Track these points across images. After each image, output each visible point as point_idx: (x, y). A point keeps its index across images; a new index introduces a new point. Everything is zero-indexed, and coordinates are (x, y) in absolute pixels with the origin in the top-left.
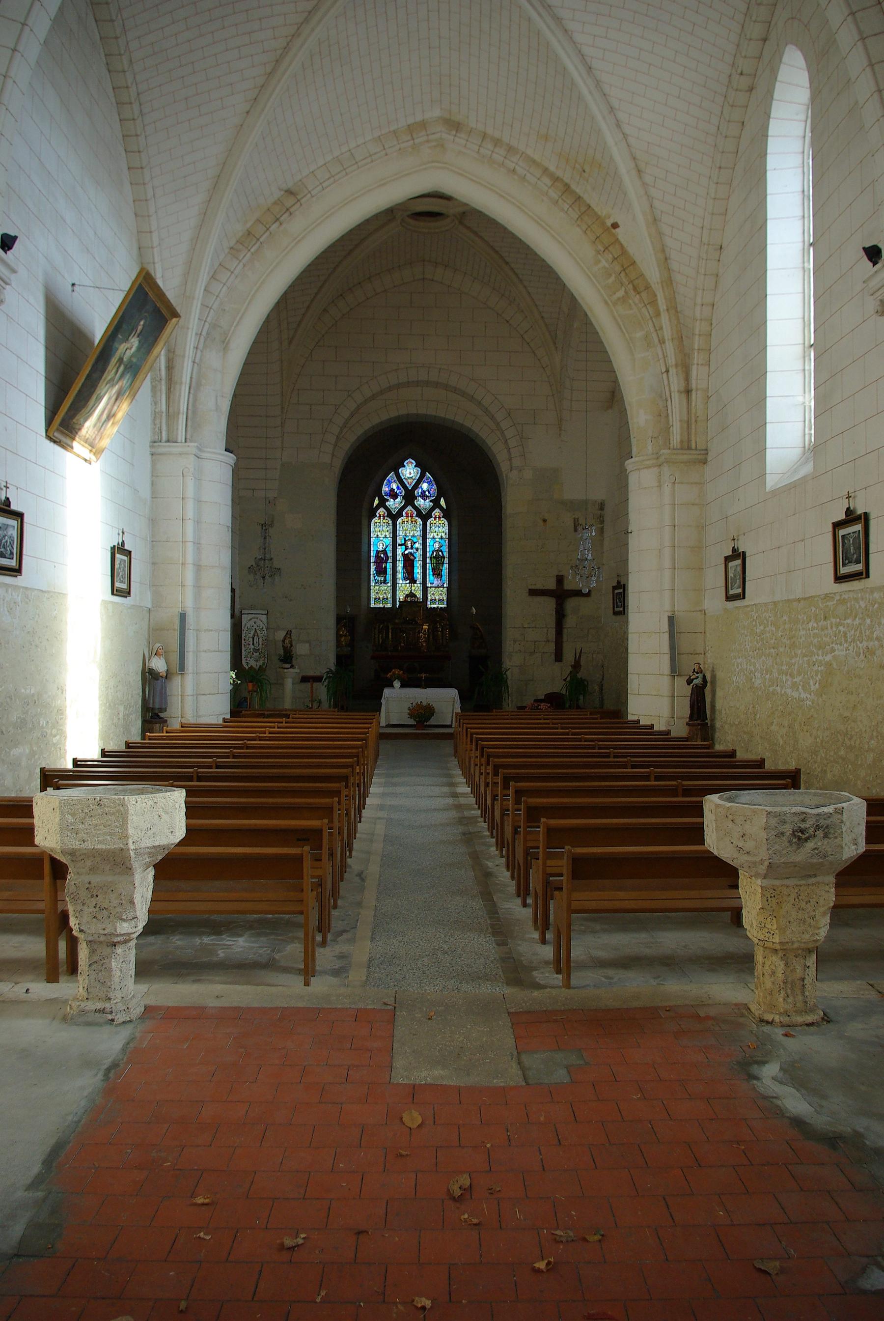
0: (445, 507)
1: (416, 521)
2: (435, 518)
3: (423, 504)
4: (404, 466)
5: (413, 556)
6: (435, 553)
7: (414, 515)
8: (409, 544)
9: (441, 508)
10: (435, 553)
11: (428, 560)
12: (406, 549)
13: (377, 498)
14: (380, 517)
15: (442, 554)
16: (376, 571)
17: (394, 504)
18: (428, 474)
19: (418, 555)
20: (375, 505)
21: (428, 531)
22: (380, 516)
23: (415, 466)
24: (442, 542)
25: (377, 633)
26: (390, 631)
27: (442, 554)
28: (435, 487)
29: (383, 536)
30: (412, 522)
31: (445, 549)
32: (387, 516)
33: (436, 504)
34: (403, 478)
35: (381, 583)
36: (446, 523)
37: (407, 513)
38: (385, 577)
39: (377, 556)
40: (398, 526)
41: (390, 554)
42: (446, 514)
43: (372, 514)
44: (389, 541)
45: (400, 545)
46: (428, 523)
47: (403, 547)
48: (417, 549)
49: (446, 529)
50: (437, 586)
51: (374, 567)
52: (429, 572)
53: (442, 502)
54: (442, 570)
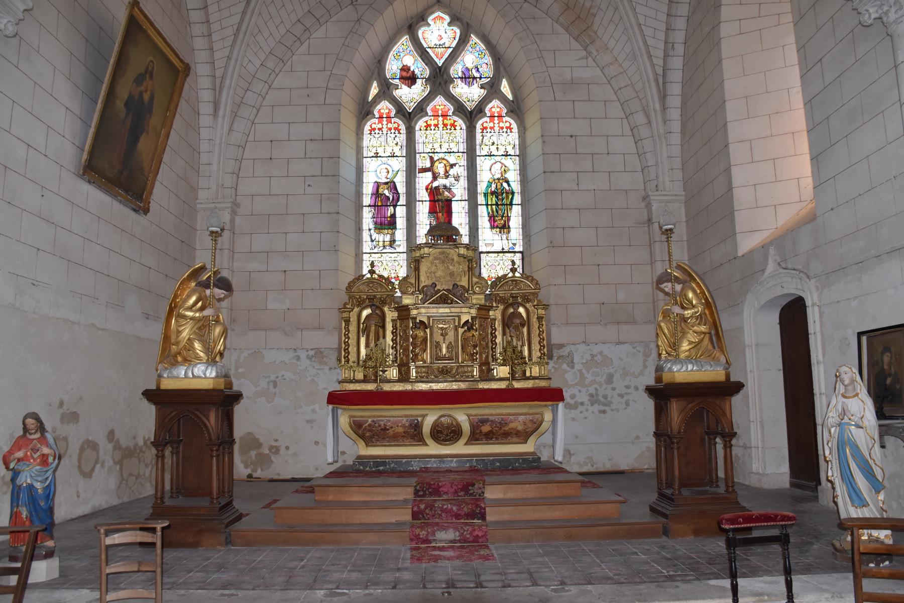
0: (510, 97)
1: (453, 125)
3: (469, 93)
4: (429, 25)
5: (449, 190)
6: (494, 186)
7: (450, 113)
8: (440, 168)
9: (503, 99)
10: (494, 186)
11: (481, 199)
13: (375, 84)
14: (381, 117)
15: (509, 185)
16: (376, 223)
17: (409, 95)
18: (474, 39)
19: (460, 190)
20: (370, 98)
21: (478, 141)
22: (381, 117)
23: (450, 24)
24: (508, 162)
25: (353, 335)
26: (389, 327)
27: (509, 185)
28: (488, 59)
29: (388, 154)
30: (445, 125)
31: (513, 176)
32: (396, 116)
33: (492, 89)
34: (425, 46)
35: (384, 247)
36: (514, 126)
37: (435, 110)
38: (393, 234)
39: (376, 194)
40: (418, 134)
41: (401, 189)
42: (515, 109)
43: (365, 111)
44: (399, 164)
46: (479, 126)
47: (429, 175)
48: (457, 178)
49: (514, 137)
50: (500, 249)
51: (371, 215)
52: (484, 221)
54: (509, 218)
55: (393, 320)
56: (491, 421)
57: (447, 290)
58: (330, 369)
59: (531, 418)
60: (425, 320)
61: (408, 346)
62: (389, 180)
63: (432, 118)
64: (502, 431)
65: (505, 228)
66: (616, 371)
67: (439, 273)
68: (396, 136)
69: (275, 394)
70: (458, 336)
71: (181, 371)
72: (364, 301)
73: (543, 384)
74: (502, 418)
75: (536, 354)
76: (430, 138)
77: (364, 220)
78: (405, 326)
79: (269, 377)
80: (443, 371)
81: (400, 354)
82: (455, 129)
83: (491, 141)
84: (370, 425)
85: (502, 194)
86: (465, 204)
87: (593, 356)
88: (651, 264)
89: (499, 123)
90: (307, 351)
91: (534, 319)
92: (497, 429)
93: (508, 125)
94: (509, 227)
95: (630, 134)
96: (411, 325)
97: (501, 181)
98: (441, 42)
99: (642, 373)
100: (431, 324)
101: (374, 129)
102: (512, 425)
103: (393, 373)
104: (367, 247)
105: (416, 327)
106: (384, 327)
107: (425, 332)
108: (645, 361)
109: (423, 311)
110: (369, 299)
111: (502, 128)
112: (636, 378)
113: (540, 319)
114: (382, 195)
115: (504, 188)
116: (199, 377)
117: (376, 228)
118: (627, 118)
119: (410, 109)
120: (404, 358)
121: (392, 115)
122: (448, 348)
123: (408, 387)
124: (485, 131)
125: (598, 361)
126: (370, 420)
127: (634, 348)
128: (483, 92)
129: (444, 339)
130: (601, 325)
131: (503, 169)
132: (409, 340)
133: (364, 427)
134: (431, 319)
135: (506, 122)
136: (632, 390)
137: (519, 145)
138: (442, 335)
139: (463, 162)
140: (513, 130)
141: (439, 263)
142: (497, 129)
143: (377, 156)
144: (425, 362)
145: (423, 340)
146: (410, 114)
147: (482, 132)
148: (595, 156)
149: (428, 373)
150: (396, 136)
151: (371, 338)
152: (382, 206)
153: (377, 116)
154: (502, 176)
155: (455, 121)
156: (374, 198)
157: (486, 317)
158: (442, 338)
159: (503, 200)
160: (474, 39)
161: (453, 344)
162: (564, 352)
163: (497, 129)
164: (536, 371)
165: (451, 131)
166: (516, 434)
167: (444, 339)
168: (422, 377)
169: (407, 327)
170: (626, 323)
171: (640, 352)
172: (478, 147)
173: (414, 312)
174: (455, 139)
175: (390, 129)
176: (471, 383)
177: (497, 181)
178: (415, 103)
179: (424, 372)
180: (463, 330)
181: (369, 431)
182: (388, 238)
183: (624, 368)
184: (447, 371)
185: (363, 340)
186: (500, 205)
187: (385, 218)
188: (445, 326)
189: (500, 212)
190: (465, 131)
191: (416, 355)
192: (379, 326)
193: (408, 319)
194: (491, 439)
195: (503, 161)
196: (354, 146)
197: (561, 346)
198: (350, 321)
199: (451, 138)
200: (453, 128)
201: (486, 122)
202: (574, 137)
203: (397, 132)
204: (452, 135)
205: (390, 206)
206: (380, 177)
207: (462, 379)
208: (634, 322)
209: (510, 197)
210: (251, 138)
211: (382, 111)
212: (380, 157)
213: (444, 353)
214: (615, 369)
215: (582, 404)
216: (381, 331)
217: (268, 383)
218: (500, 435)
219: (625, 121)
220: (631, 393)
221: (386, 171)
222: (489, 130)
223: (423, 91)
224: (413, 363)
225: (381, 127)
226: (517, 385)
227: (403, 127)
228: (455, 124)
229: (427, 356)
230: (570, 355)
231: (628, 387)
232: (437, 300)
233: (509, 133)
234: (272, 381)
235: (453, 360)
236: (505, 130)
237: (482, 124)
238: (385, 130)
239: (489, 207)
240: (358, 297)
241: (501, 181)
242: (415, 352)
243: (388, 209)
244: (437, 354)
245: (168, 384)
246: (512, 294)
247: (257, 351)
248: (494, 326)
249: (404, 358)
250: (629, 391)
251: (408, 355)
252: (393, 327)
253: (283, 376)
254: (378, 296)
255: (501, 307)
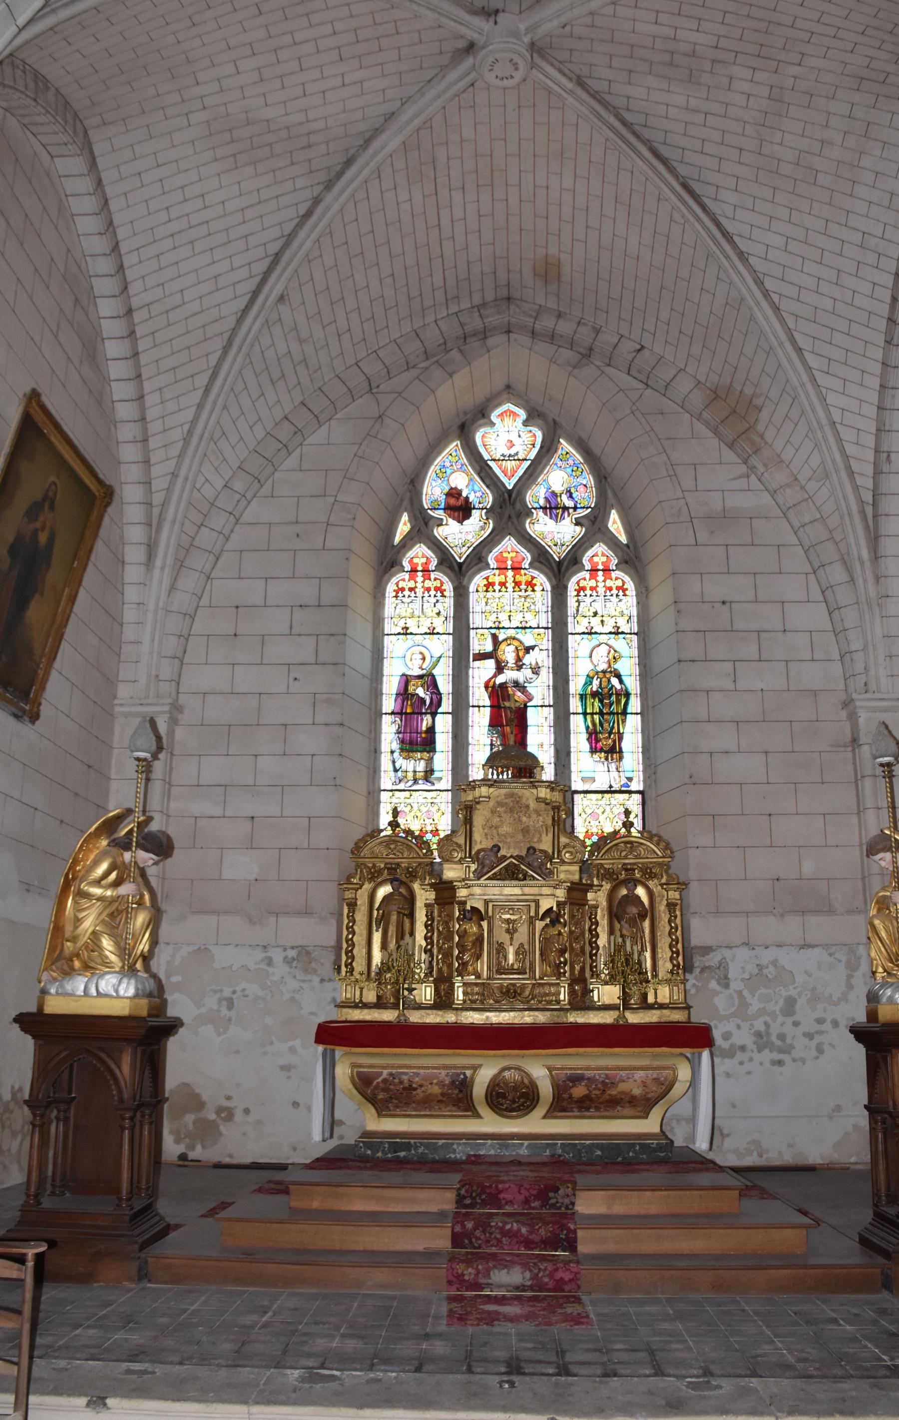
0: (623, 538)
1: (531, 584)
2: (594, 571)
4: (493, 424)
6: (596, 683)
8: (508, 654)
9: (612, 542)
10: (596, 683)
11: (575, 705)
12: (500, 669)
13: (405, 517)
14: (414, 571)
15: (621, 682)
16: (402, 742)
18: (565, 446)
20: (397, 539)
21: (571, 610)
22: (414, 571)
23: (526, 423)
24: (620, 644)
25: (360, 928)
27: (621, 682)
28: (588, 479)
30: (517, 584)
31: (629, 668)
32: (437, 568)
34: (486, 456)
35: (415, 781)
36: (630, 585)
37: (500, 560)
38: (430, 761)
39: (404, 694)
40: (473, 597)
41: (445, 686)
44: (443, 646)
45: (482, 656)
46: (572, 586)
47: (491, 664)
48: (536, 670)
49: (629, 604)
50: (605, 787)
51: (394, 728)
52: (579, 741)
53: (615, 524)
54: (620, 736)
55: (427, 905)
56: (589, 1079)
57: (519, 858)
58: (322, 981)
59: (655, 1076)
60: (480, 906)
61: (451, 948)
62: (424, 672)
63: (497, 572)
64: (606, 1097)
65: (614, 752)
66: (800, 994)
67: (505, 829)
68: (437, 601)
69: (230, 1019)
70: (534, 934)
71: (78, 984)
72: (380, 872)
73: (677, 1016)
74: (607, 1075)
75: (665, 966)
76: (493, 606)
77: (383, 737)
78: (448, 915)
79: (221, 991)
80: (508, 991)
81: (438, 961)
82: (533, 590)
83: (593, 610)
84: (385, 1081)
85: (611, 695)
86: (549, 713)
87: (760, 967)
88: (859, 813)
89: (605, 581)
90: (285, 950)
91: (662, 907)
92: (598, 1092)
93: (619, 583)
94: (621, 751)
95: (822, 599)
96: (457, 914)
97: (608, 675)
98: (513, 451)
99: (844, 998)
100: (490, 914)
101: (403, 589)
102: (622, 1087)
103: (426, 993)
104: (387, 780)
105: (465, 917)
106: (411, 916)
107: (480, 926)
108: (849, 977)
109: (477, 890)
110: (388, 869)
111: (610, 589)
112: (835, 1005)
113: (671, 906)
114: (413, 695)
115: (613, 686)
116: (107, 996)
117: (402, 750)
118: (814, 573)
119: (460, 558)
120: (445, 969)
121: (432, 566)
122: (517, 953)
123: (450, 1017)
124: (582, 593)
125: (770, 976)
126: (385, 1073)
127: (830, 955)
128: (579, 531)
129: (512, 939)
130: (775, 915)
131: (611, 656)
132: (453, 939)
133: (375, 1083)
134: (490, 905)
135: (617, 579)
136: (827, 1026)
137: (638, 616)
138: (508, 931)
139: (546, 642)
140: (627, 592)
141: (505, 812)
142: (601, 590)
143: (406, 632)
144: (478, 976)
145: (477, 939)
146: (460, 565)
147: (578, 595)
148: (763, 635)
149: (483, 995)
150: (437, 601)
151: (390, 933)
152: (413, 713)
153: (407, 567)
154: (610, 666)
155: (533, 578)
156: (399, 701)
157: (581, 902)
158: (508, 936)
159: (611, 705)
160: (565, 446)
161: (526, 947)
162: (713, 959)
163: (601, 590)
164: (664, 994)
165: (527, 593)
166: (630, 1102)
167: (512, 939)
168: (473, 1002)
169: (450, 916)
170: (818, 912)
171: (840, 961)
172: (570, 619)
173: (462, 893)
174: (533, 607)
175: (428, 589)
176: (555, 1013)
177: (601, 675)
178: (469, 548)
179: (477, 994)
180: (543, 923)
181: (384, 1090)
182: (421, 766)
183: (814, 989)
184: (515, 992)
185: (377, 937)
186: (607, 714)
187: (417, 733)
188: (513, 917)
189: (606, 725)
190: (549, 593)
191: (464, 965)
192: (404, 915)
193: (452, 903)
194: (587, 1109)
195: (612, 642)
196: (370, 617)
197: (707, 950)
198: (356, 905)
199: (526, 604)
200: (530, 588)
201: (585, 579)
202: (728, 604)
203: (439, 594)
204: (528, 600)
205: (426, 713)
206: (411, 666)
207: (540, 1006)
208: (831, 912)
209: (623, 701)
210: (204, 601)
211: (415, 560)
212: (411, 634)
213: (511, 962)
214: (798, 990)
215: (743, 1048)
216: (407, 922)
217: (220, 1001)
218: (601, 1103)
219: (812, 577)
220: (827, 1032)
221: (421, 657)
222: (588, 592)
223: (483, 528)
224: (460, 978)
225: (413, 586)
226: (633, 1018)
227: (448, 587)
228: (534, 582)
229: (483, 965)
230: (723, 965)
231: (820, 1021)
232: (500, 874)
233: (621, 597)
234: (225, 999)
235: (526, 973)
236: (614, 592)
237: (578, 583)
238: (419, 591)
239: (589, 717)
240: (370, 865)
241: (608, 675)
242: (462, 958)
243: (422, 720)
244: (499, 963)
245: (55, 1005)
246: (625, 864)
247: (203, 947)
248: (595, 918)
249: (445, 969)
250: (823, 1027)
251: (451, 964)
252: (427, 916)
253: (244, 990)
254: (403, 865)
255: (607, 886)
